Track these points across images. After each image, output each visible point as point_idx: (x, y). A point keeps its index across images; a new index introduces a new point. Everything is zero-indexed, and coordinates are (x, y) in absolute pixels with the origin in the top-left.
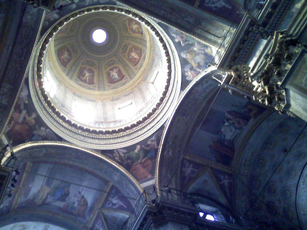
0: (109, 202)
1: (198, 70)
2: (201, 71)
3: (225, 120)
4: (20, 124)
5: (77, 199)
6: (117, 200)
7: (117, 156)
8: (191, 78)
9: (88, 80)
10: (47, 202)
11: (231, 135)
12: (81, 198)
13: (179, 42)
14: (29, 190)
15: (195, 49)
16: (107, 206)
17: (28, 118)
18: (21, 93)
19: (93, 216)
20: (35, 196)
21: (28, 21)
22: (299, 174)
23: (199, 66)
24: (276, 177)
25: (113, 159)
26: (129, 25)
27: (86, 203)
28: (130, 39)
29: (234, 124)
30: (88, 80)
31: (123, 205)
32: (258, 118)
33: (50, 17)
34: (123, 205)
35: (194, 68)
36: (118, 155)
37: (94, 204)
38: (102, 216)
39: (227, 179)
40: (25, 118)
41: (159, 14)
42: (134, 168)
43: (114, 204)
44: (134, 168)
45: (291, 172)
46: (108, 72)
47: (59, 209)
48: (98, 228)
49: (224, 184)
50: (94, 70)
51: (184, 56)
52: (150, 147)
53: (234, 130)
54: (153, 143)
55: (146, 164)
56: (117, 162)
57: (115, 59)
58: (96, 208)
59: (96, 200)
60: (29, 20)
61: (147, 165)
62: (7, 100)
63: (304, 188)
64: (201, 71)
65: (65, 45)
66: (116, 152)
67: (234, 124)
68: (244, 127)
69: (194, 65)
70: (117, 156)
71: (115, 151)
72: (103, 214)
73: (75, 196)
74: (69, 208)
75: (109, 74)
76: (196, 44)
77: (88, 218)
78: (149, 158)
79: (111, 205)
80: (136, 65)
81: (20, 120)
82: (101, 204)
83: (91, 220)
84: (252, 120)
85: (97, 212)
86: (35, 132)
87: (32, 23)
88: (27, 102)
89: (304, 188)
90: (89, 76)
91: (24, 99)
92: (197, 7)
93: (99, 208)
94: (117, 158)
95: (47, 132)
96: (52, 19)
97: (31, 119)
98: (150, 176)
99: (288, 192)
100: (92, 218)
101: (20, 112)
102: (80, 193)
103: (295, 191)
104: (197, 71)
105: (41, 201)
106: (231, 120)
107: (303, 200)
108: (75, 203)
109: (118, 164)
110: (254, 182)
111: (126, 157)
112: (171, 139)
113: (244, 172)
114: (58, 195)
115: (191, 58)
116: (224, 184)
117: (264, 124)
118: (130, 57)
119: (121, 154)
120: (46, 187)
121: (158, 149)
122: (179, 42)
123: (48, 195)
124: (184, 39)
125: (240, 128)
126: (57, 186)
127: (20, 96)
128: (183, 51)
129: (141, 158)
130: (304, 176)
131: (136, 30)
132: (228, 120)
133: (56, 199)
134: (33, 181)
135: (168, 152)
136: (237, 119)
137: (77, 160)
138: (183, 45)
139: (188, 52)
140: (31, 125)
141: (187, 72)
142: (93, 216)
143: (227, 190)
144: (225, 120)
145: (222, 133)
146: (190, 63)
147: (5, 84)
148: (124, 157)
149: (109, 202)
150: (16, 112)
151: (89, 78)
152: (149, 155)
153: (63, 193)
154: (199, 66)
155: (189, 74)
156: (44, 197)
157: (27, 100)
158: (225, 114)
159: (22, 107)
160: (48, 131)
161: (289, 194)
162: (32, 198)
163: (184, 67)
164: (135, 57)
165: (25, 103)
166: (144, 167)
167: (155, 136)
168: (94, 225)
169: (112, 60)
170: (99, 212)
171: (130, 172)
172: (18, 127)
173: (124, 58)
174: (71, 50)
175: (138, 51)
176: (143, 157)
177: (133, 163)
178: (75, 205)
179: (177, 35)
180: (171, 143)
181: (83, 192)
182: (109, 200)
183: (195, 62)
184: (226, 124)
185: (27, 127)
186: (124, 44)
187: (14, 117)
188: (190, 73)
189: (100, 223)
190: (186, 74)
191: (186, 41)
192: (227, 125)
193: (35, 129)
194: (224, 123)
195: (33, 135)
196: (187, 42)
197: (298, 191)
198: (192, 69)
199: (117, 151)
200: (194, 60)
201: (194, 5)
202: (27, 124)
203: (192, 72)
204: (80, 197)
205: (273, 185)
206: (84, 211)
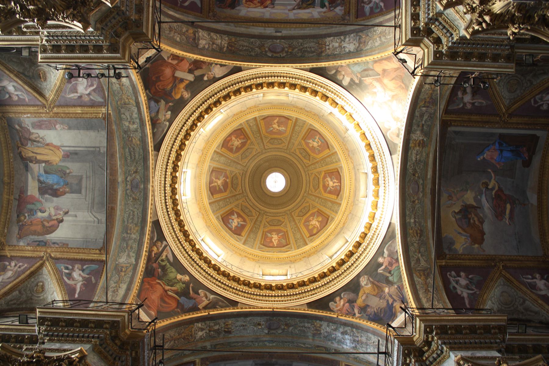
0: (70, 267)
1: (356, 311)
2: (357, 315)
4: (173, 76)
5: (53, 212)
6: (81, 279)
7: (158, 249)
8: (335, 309)
9: (213, 185)
10: (31, 164)
12: (57, 219)
13: (380, 265)
14: (50, 126)
15: (387, 290)
16: (62, 267)
17: (182, 86)
18: (219, 66)
19: (28, 251)
20: (38, 142)
21: (328, 46)
23: (363, 309)
25: (152, 244)
26: (313, 215)
27: (52, 229)
28: (293, 223)
30: (213, 185)
31: (78, 290)
33: (343, 73)
34: (78, 290)
35: (355, 304)
36: (161, 249)
37: (54, 243)
38: (38, 264)
40: (182, 80)
41: (407, 218)
42: (152, 283)
43: (69, 276)
44: (152, 283)
46: (233, 211)
47: (23, 191)
48: (9, 267)
50: (228, 191)
51: (363, 281)
52: (195, 296)
54: (204, 299)
55: (167, 300)
56: (150, 252)
57: (254, 214)
58: (49, 251)
59: (64, 245)
60: (331, 46)
61: (165, 302)
62: (207, 47)
64: (357, 315)
65: (250, 139)
66: (163, 246)
69: (360, 301)
70: (158, 249)
71: (165, 243)
72: (42, 266)
73: (57, 208)
74: (30, 206)
75: (231, 213)
76: (396, 286)
77: (21, 244)
78: (178, 302)
79: (67, 271)
80: (263, 245)
81: (179, 74)
82: (58, 255)
83: (23, 251)
85: (42, 254)
86: (163, 102)
87: (328, 51)
88: (205, 78)
90: (219, 186)
91: (210, 73)
92: (439, 264)
93: (50, 255)
94: (155, 249)
95: (165, 123)
96: (340, 77)
97: (182, 92)
100: (26, 251)
101: (190, 71)
102: (66, 213)
104: (354, 310)
105: (31, 155)
108: (44, 212)
109: (147, 254)
111: (164, 264)
112: (223, 325)
114: (51, 180)
115: (367, 292)
118: (269, 235)
119: (165, 254)
120: (61, 154)
121: (198, 309)
122: (380, 265)
123: (46, 162)
124: (390, 268)
126: (68, 171)
127: (213, 65)
128: (370, 276)
129: (173, 288)
131: (310, 227)
133: (42, 179)
134: (70, 128)
135: (202, 330)
137: (129, 187)
138: (380, 270)
139: (373, 283)
140: (173, 94)
141: (341, 298)
142: (28, 251)
146: (358, 295)
147: (227, 38)
148: (162, 260)
149: (70, 267)
150: (190, 65)
151: (216, 186)
152: (182, 300)
153: (55, 187)
154: (363, 309)
155: (340, 303)
156: (39, 157)
157: (208, 77)
159: (198, 73)
160: (166, 125)
162: (33, 137)
163: (345, 291)
164: (273, 240)
165: (203, 75)
166: (162, 299)
167: (215, 298)
168: (12, 258)
169: (250, 211)
170: (43, 257)
171: (143, 278)
172: (168, 72)
173: (262, 227)
174: (244, 148)
175: (283, 241)
176: (176, 290)
178: (40, 214)
179: (389, 255)
180: (217, 327)
181: (70, 218)
182: (73, 267)
183: (364, 300)
185: (169, 88)
186: (280, 218)
187: (183, 62)
188: (342, 302)
189: (19, 267)
190: (338, 299)
191: (390, 272)
193: (167, 103)
195: (157, 102)
196: (388, 275)
198: (351, 302)
199: (166, 246)
200: (367, 297)
201: (438, 259)
202: (174, 87)
203: (347, 304)
204: (59, 217)
206: (35, 233)
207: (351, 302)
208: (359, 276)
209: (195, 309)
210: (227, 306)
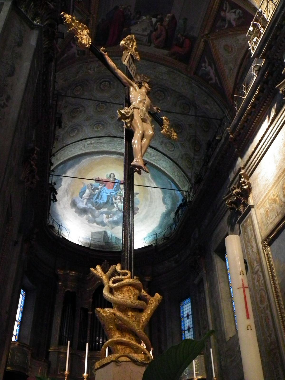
3: (159, 17)
11: (138, 32)
22: (100, 135)
24: (91, 111)
29: (156, 30)
32: (170, 58)
39: (78, 51)
45: (100, 125)
49: (72, 47)
53: (146, 33)
63: (84, 146)
67: (156, 30)
68: (153, 45)
84: (166, 52)
89: (84, 146)
99: (76, 132)
103: (79, 140)
106: (161, 25)
107: (72, 151)
110: (80, 87)
113: (90, 69)
116: (72, 47)
117: (163, 69)
125: (150, 41)
130: (98, 141)
132: (161, 20)
136: (164, 33)
143: (66, 55)
144: (159, 17)
145: (139, 18)
158: (170, 13)
161: (74, 134)
184: (154, 20)
192: (152, 22)
194: (155, 17)
197: (79, 143)
205: (81, 112)
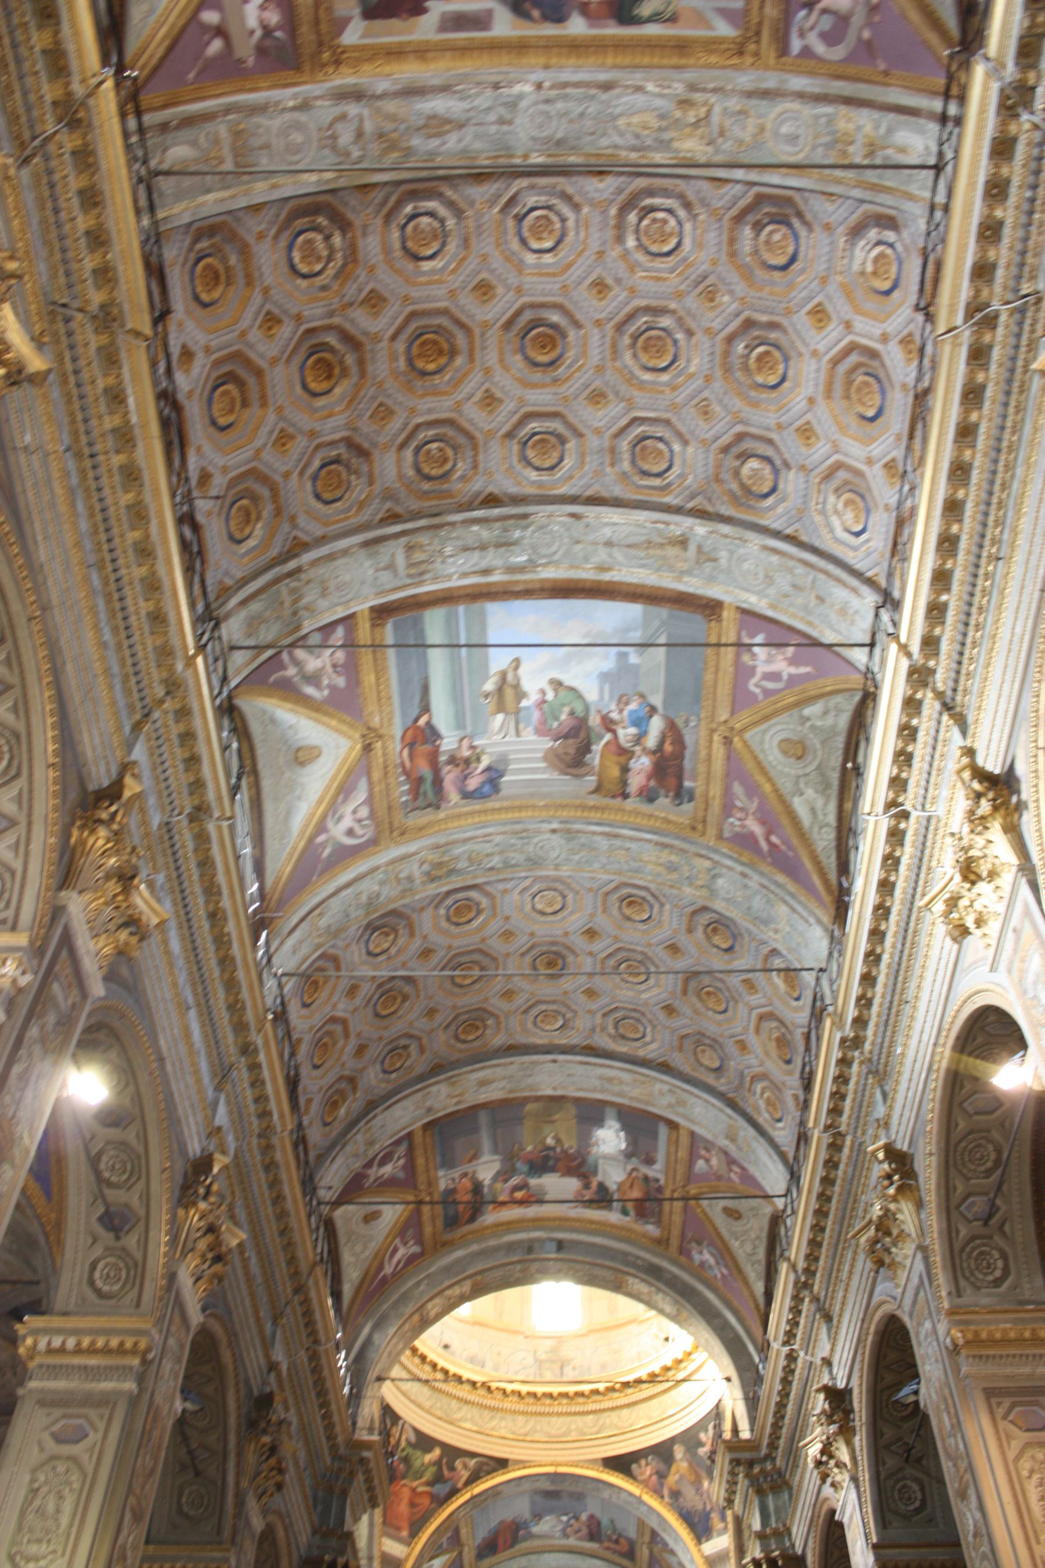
1: (666, 1492)
8: (641, 1478)
23: (676, 1494)
51: (679, 1452)
55: (417, 1501)
64: (667, 1499)
69: (672, 1479)
98: (405, 1533)
155: (646, 1469)
166: (412, 1504)
177: (404, 1477)
184: (564, 1518)
190: (643, 1462)
203: (654, 1478)
207: (662, 1476)
208: (672, 1441)
209: (454, 1492)
210: (494, 1470)
